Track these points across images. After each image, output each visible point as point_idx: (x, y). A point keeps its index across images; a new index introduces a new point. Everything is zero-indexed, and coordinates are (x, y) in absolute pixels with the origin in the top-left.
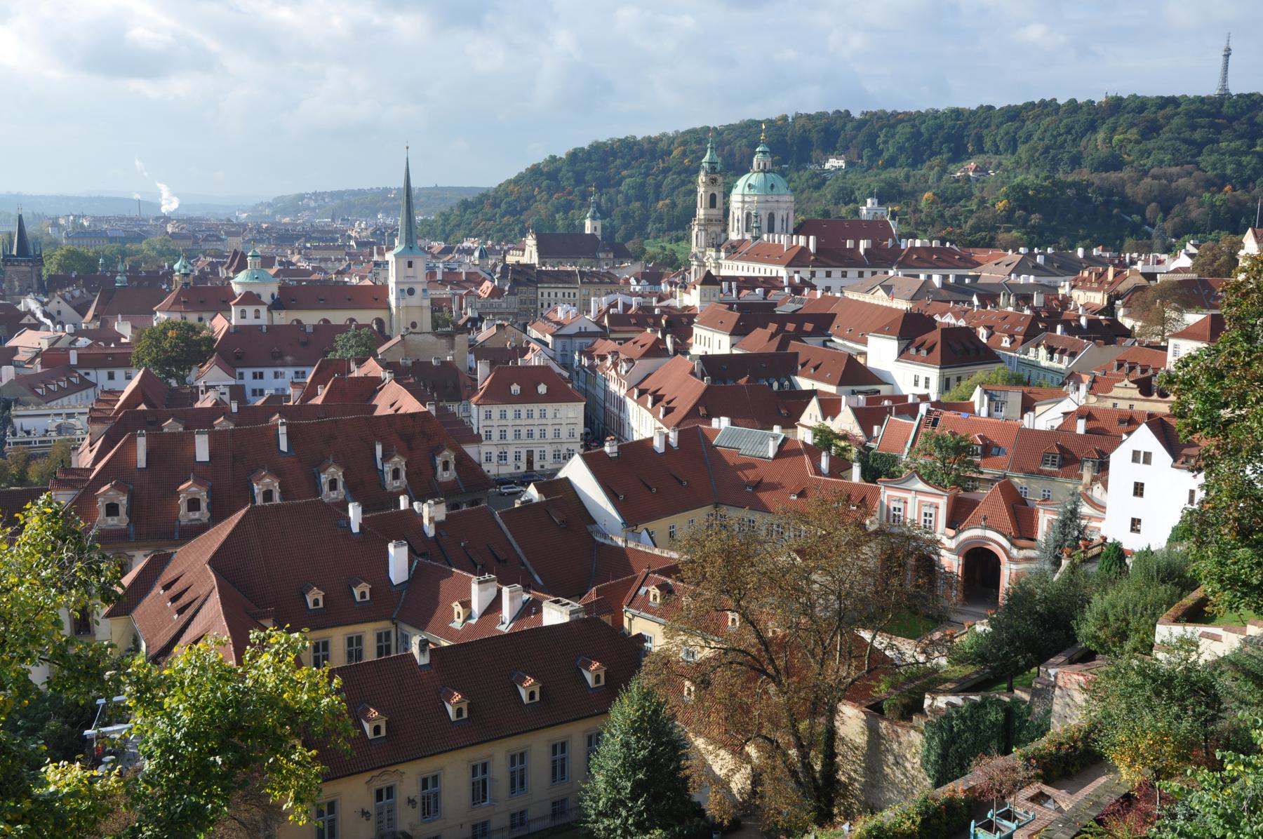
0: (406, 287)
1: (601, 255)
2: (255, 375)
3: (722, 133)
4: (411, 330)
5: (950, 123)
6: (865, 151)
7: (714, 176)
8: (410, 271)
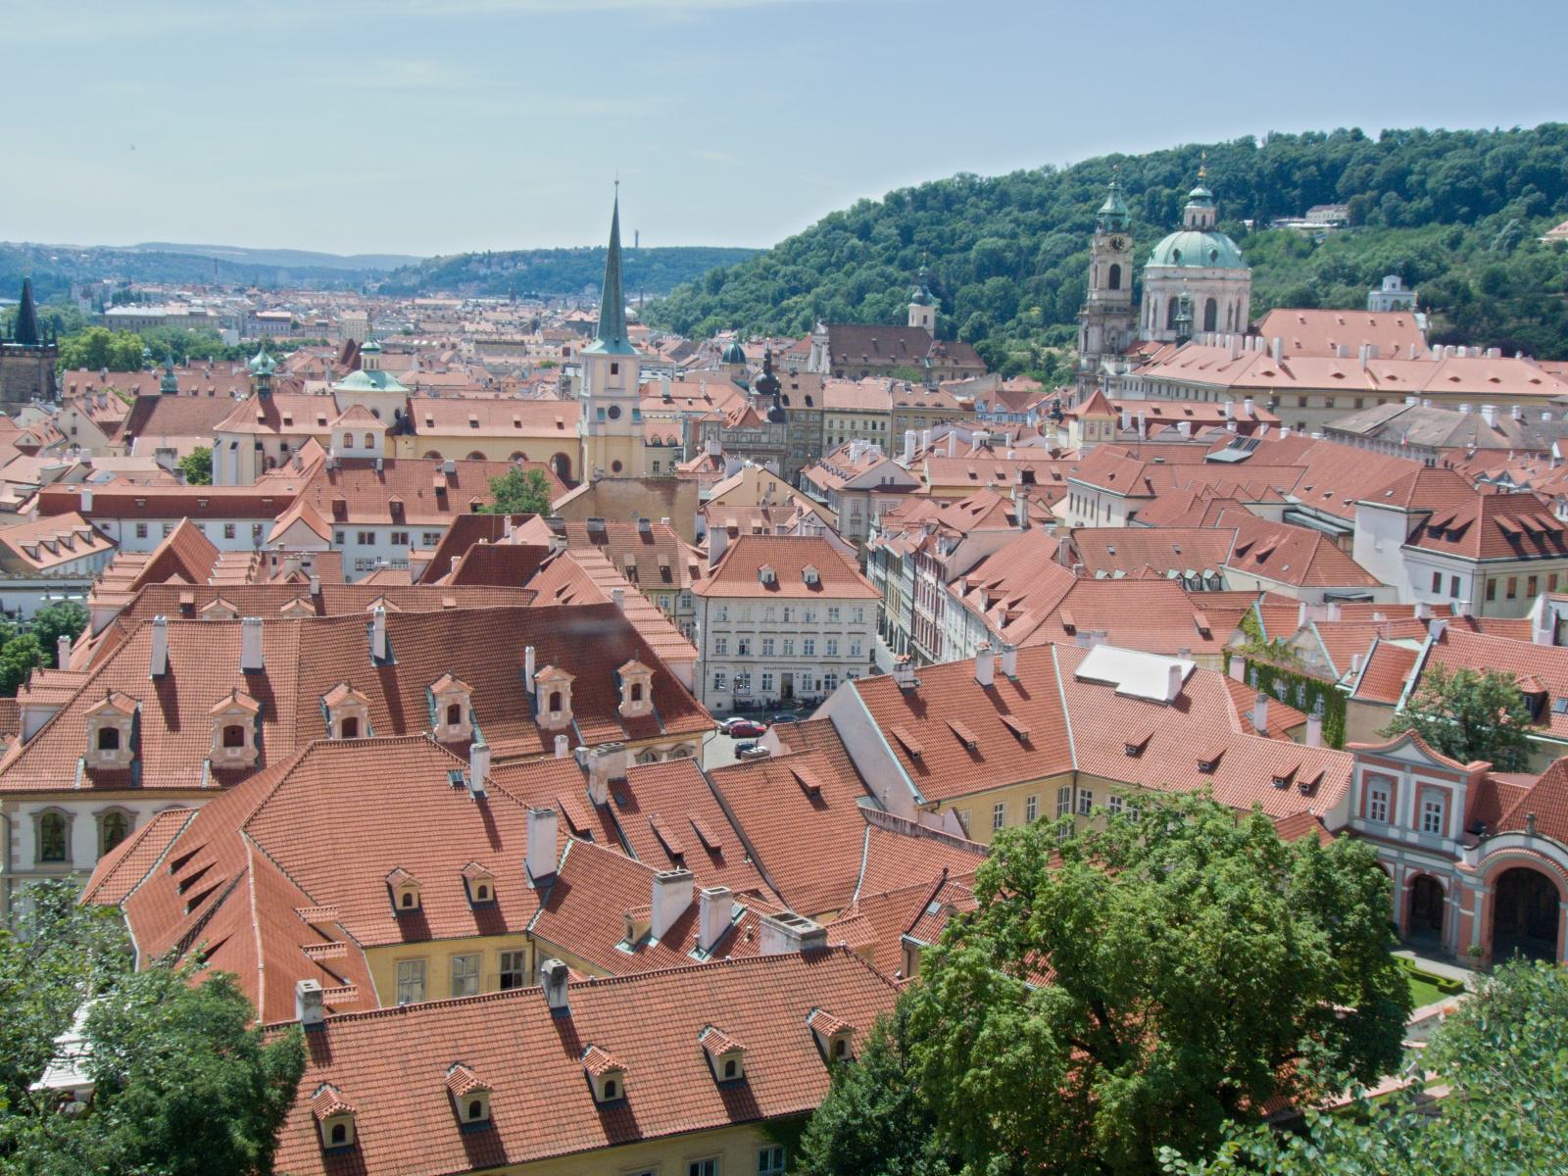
0: (606, 405)
2: (361, 541)
4: (611, 473)
5: (1536, 151)
8: (615, 381)
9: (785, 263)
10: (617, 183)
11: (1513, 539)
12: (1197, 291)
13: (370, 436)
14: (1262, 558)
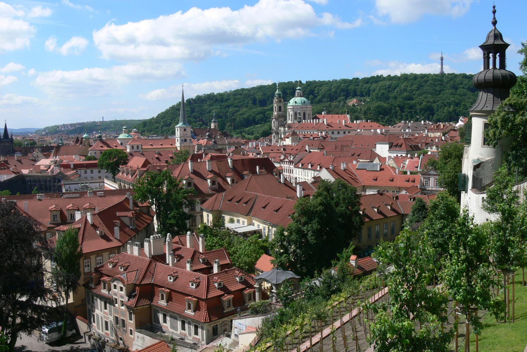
0: (183, 139)
3: (250, 91)
5: (343, 85)
6: (310, 96)
9: (162, 119)
11: (411, 146)
13: (138, 146)
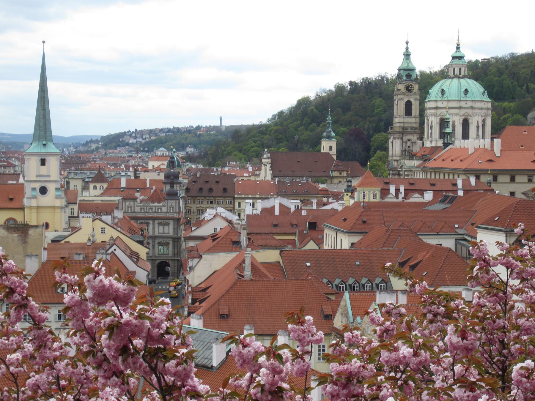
0: (38, 186)
1: (336, 174)
7: (409, 83)
8: (43, 170)
10: (44, 42)
12: (456, 115)
14: (413, 267)
